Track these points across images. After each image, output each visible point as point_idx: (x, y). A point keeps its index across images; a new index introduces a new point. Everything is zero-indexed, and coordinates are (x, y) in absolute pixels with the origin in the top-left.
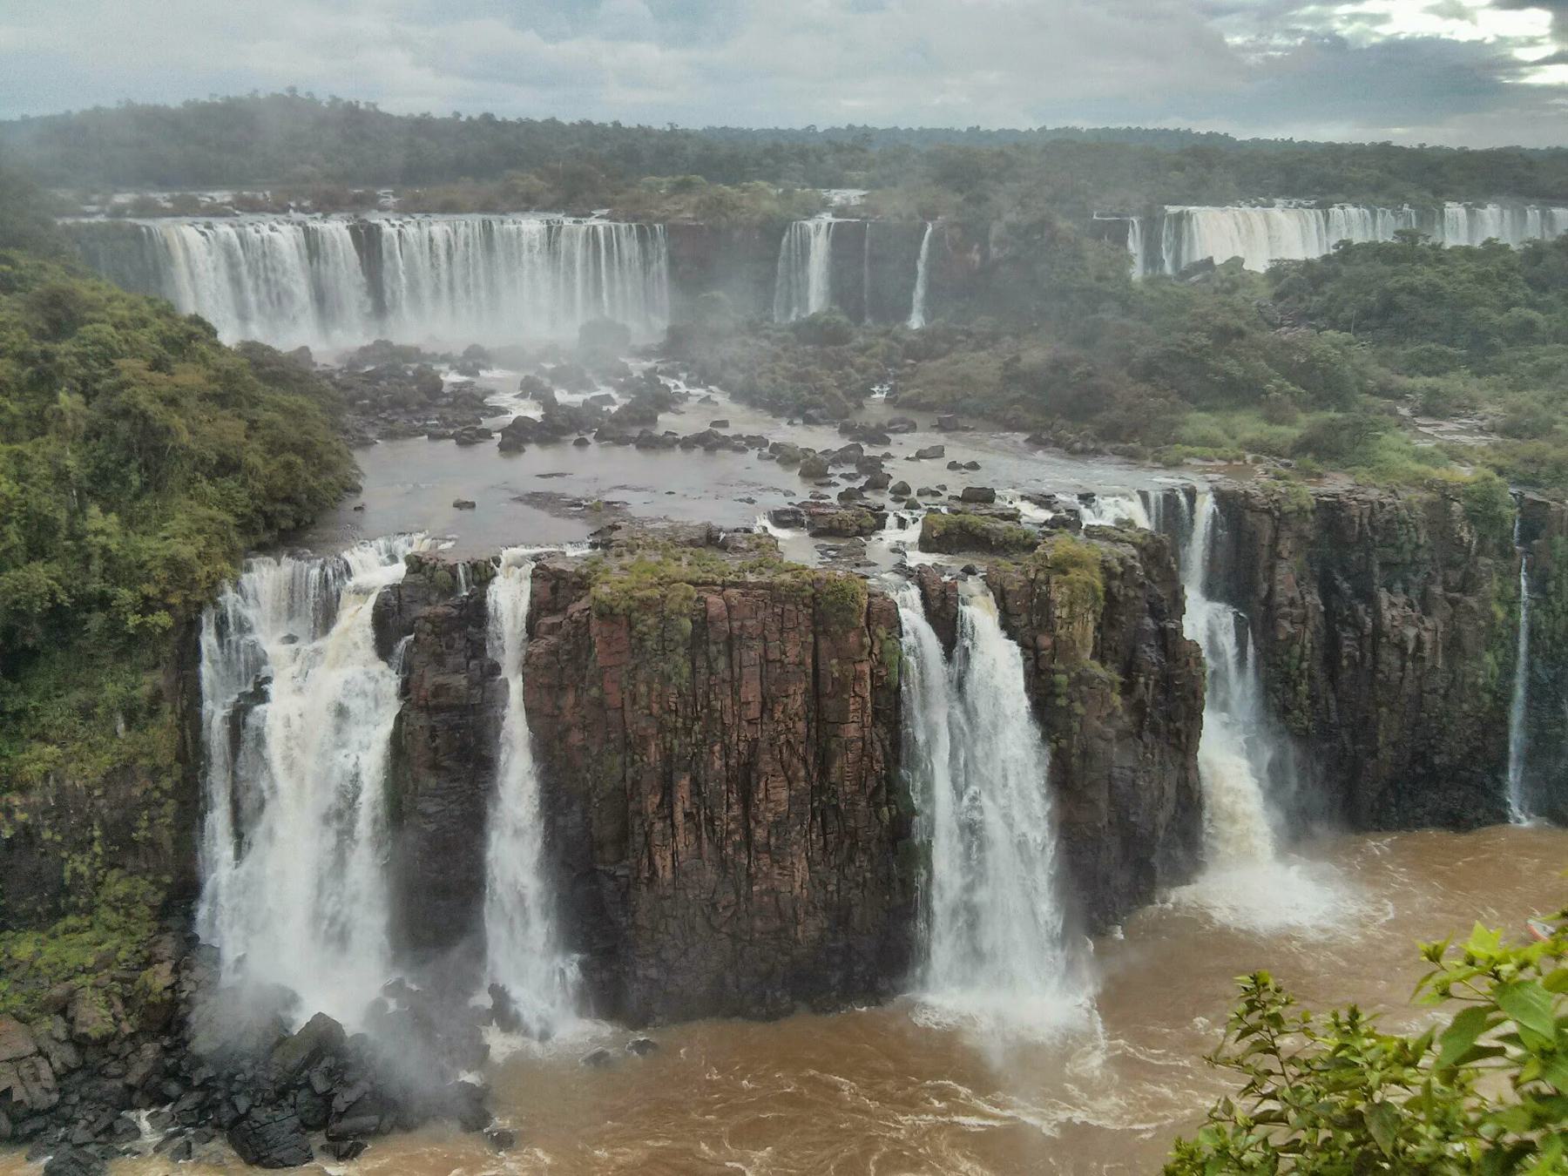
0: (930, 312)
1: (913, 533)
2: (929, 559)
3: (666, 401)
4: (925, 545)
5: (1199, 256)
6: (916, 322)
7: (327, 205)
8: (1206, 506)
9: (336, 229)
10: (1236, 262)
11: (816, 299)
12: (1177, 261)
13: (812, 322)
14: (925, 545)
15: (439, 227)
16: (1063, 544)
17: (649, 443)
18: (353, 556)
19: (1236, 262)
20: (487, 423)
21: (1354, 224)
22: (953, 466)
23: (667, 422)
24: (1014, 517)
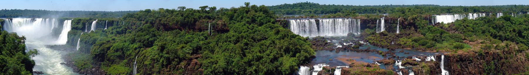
0: (400, 31)
1: (400, 63)
2: (403, 67)
3: (361, 45)
4: (402, 65)
5: (438, 22)
6: (398, 32)
7: (312, 17)
8: (443, 57)
9: (313, 21)
10: (443, 22)
11: (383, 29)
12: (434, 22)
13: (382, 33)
14: (402, 65)
15: (328, 20)
16: (423, 64)
17: (358, 51)
18: (315, 67)
19: (443, 22)
20: (334, 48)
21: (457, 17)
22: (405, 53)
23: (360, 48)
24: (415, 60)
